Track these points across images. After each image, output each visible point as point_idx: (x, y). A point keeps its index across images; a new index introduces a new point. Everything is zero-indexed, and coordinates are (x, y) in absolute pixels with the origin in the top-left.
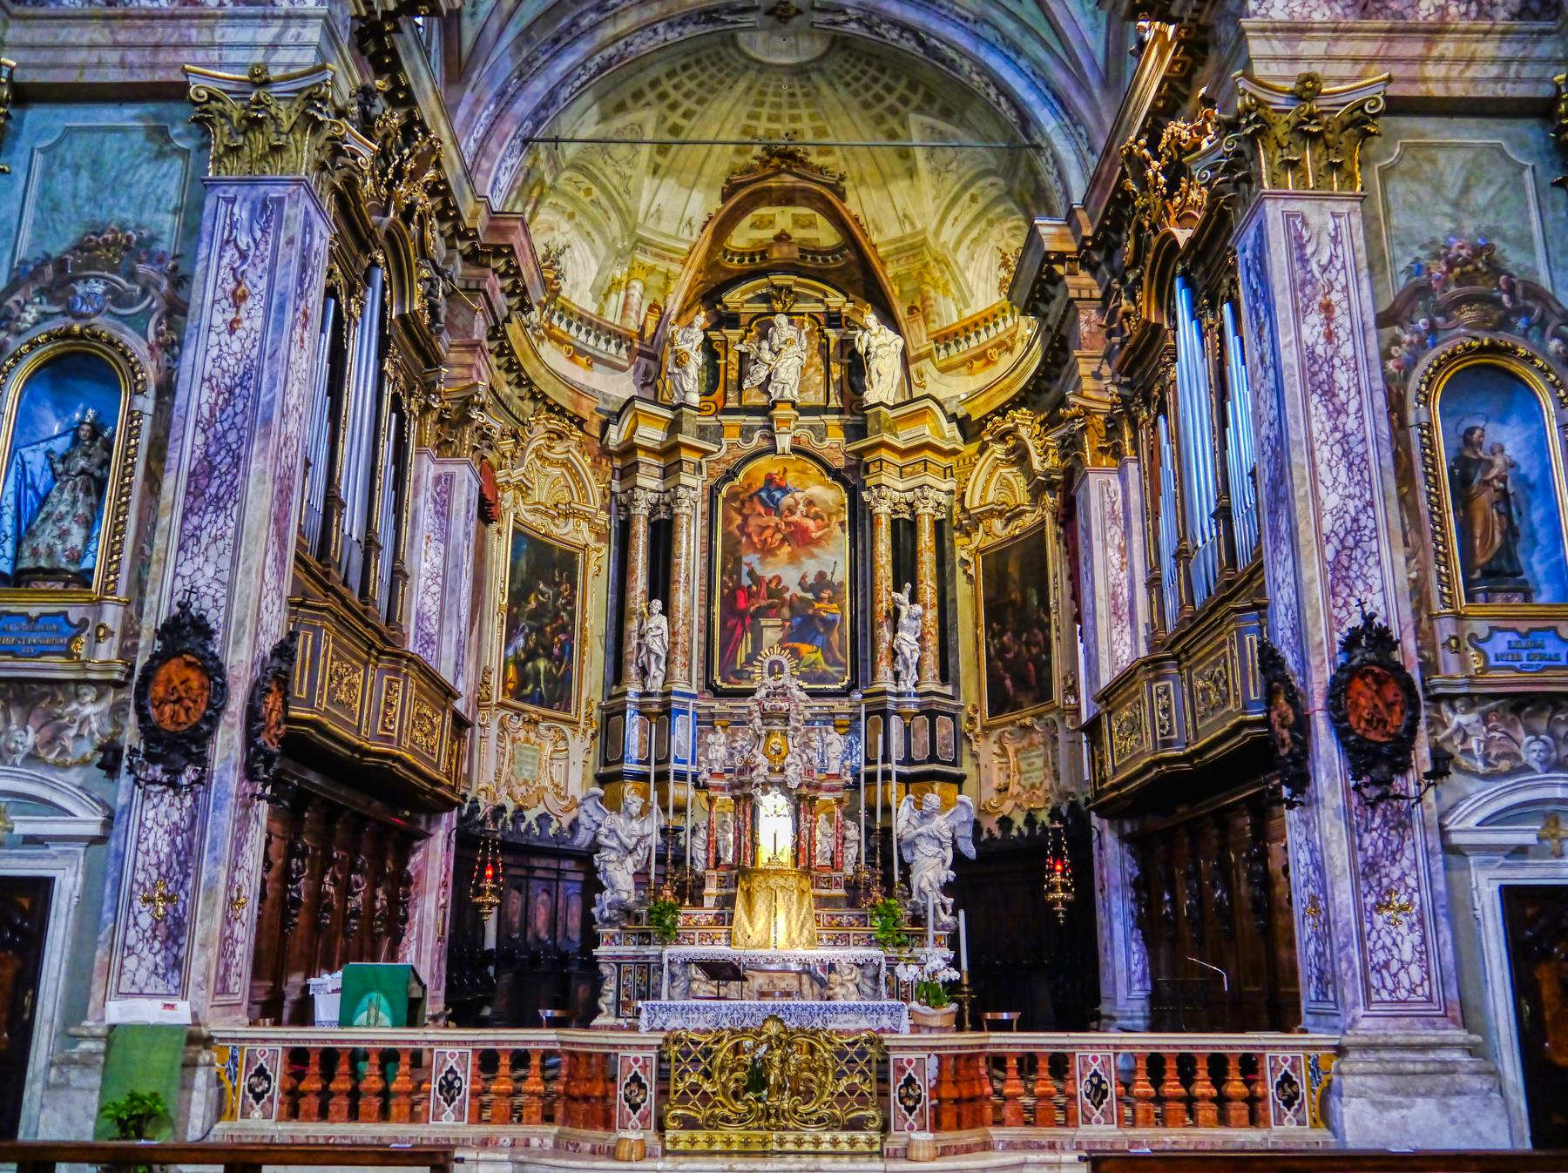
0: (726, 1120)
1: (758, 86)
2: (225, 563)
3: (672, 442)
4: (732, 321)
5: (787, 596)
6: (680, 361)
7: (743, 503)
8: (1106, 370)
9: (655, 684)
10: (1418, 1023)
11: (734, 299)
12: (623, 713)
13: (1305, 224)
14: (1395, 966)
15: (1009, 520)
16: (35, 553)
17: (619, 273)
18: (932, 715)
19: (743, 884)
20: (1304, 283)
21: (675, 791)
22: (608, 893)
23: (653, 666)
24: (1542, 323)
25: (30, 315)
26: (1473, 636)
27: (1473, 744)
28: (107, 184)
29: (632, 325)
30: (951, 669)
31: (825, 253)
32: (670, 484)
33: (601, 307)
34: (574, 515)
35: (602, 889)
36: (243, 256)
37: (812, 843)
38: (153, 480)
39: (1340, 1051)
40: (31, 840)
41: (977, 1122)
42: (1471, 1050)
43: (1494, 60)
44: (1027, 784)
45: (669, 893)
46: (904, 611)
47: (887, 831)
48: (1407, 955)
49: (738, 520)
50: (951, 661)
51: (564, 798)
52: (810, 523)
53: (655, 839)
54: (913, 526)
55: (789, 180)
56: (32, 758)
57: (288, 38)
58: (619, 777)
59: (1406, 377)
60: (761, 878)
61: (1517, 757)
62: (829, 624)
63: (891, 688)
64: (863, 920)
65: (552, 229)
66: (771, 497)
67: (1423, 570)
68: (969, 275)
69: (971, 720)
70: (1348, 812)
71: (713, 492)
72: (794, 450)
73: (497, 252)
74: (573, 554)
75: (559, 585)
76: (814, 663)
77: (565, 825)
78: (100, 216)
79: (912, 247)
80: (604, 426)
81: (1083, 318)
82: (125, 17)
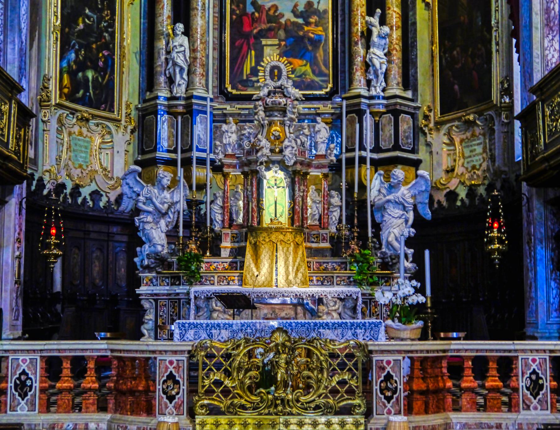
0: (243, 407)
5: (283, 21)
9: (180, 90)
12: (156, 113)
18: (395, 113)
19: (251, 239)
21: (197, 173)
22: (147, 246)
23: (178, 76)
30: (411, 78)
35: (141, 243)
37: (304, 208)
41: (440, 409)
44: (469, 166)
45: (193, 246)
46: (375, 31)
50: (412, 72)
51: (111, 178)
53: (182, 206)
58: (154, 162)
60: (265, 234)
62: (316, 43)
63: (364, 92)
64: (344, 265)
69: (426, 117)
76: (304, 74)
77: (113, 199)
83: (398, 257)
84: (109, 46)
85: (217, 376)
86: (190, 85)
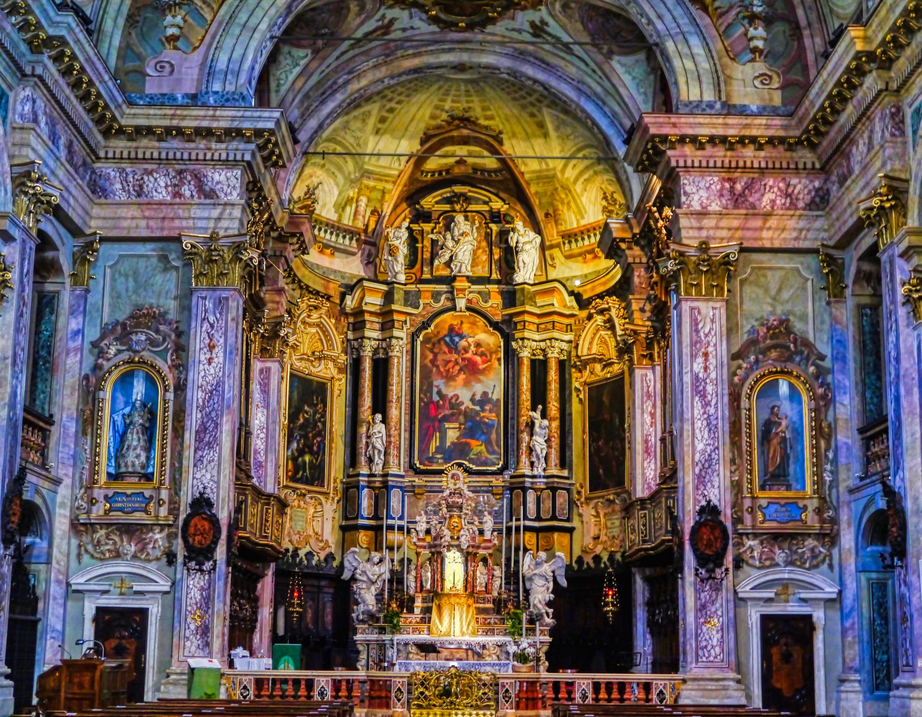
1: (446, 87)
2: (215, 473)
3: (387, 309)
4: (425, 216)
5: (463, 408)
6: (392, 252)
7: (434, 344)
8: (648, 307)
9: (378, 469)
10: (717, 671)
11: (429, 202)
13: (699, 313)
14: (709, 647)
15: (605, 366)
16: (126, 465)
17: (352, 193)
18: (554, 489)
19: (436, 601)
20: (696, 343)
22: (361, 606)
24: (808, 358)
25: (112, 351)
26: (760, 506)
27: (755, 554)
28: (142, 285)
29: (360, 225)
31: (489, 171)
32: (387, 334)
33: (340, 216)
34: (325, 358)
35: (357, 604)
36: (212, 326)
37: (474, 578)
38: (179, 432)
39: (684, 681)
40: (137, 593)
41: (535, 707)
42: (738, 682)
43: (795, 229)
46: (537, 423)
47: (517, 573)
48: (715, 642)
49: (431, 356)
50: (568, 454)
52: (478, 359)
53: (387, 576)
54: (544, 363)
55: (465, 132)
56: (135, 557)
57: (226, 215)
58: (357, 528)
59: (743, 385)
61: (773, 559)
62: (490, 426)
63: (527, 472)
64: (502, 621)
65: (311, 176)
66: (452, 341)
67: (741, 476)
68: (584, 199)
69: (579, 493)
70: (695, 584)
71: (413, 337)
72: (468, 309)
73: (293, 235)
74: (324, 384)
75: (316, 405)
76: (480, 452)
77: (322, 558)
78: (140, 301)
79: (547, 177)
80: (343, 296)
81: (636, 274)
82: (148, 204)
83: (542, 615)
84: (321, 434)
85: (421, 690)
86: (386, 464)
